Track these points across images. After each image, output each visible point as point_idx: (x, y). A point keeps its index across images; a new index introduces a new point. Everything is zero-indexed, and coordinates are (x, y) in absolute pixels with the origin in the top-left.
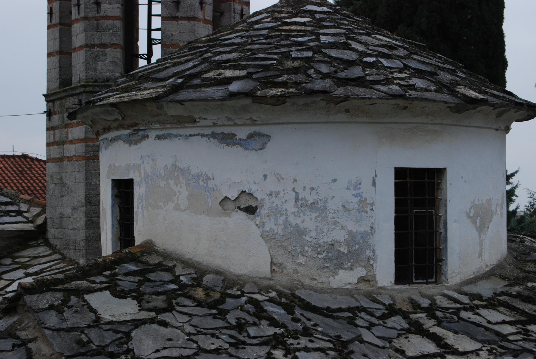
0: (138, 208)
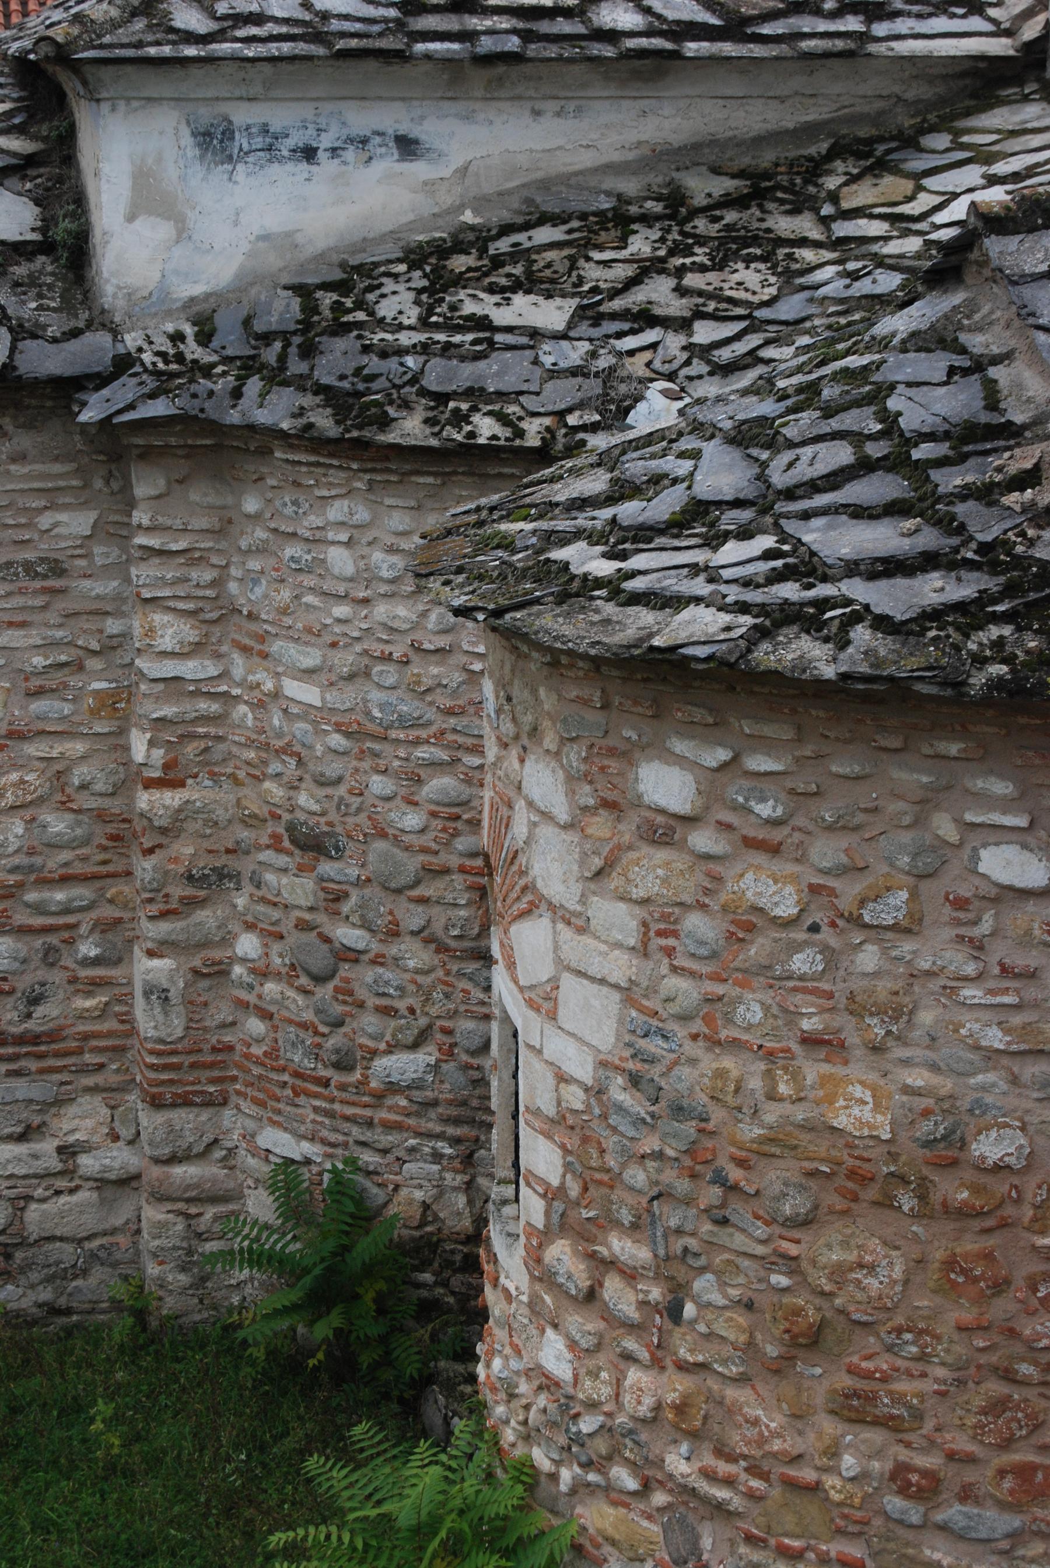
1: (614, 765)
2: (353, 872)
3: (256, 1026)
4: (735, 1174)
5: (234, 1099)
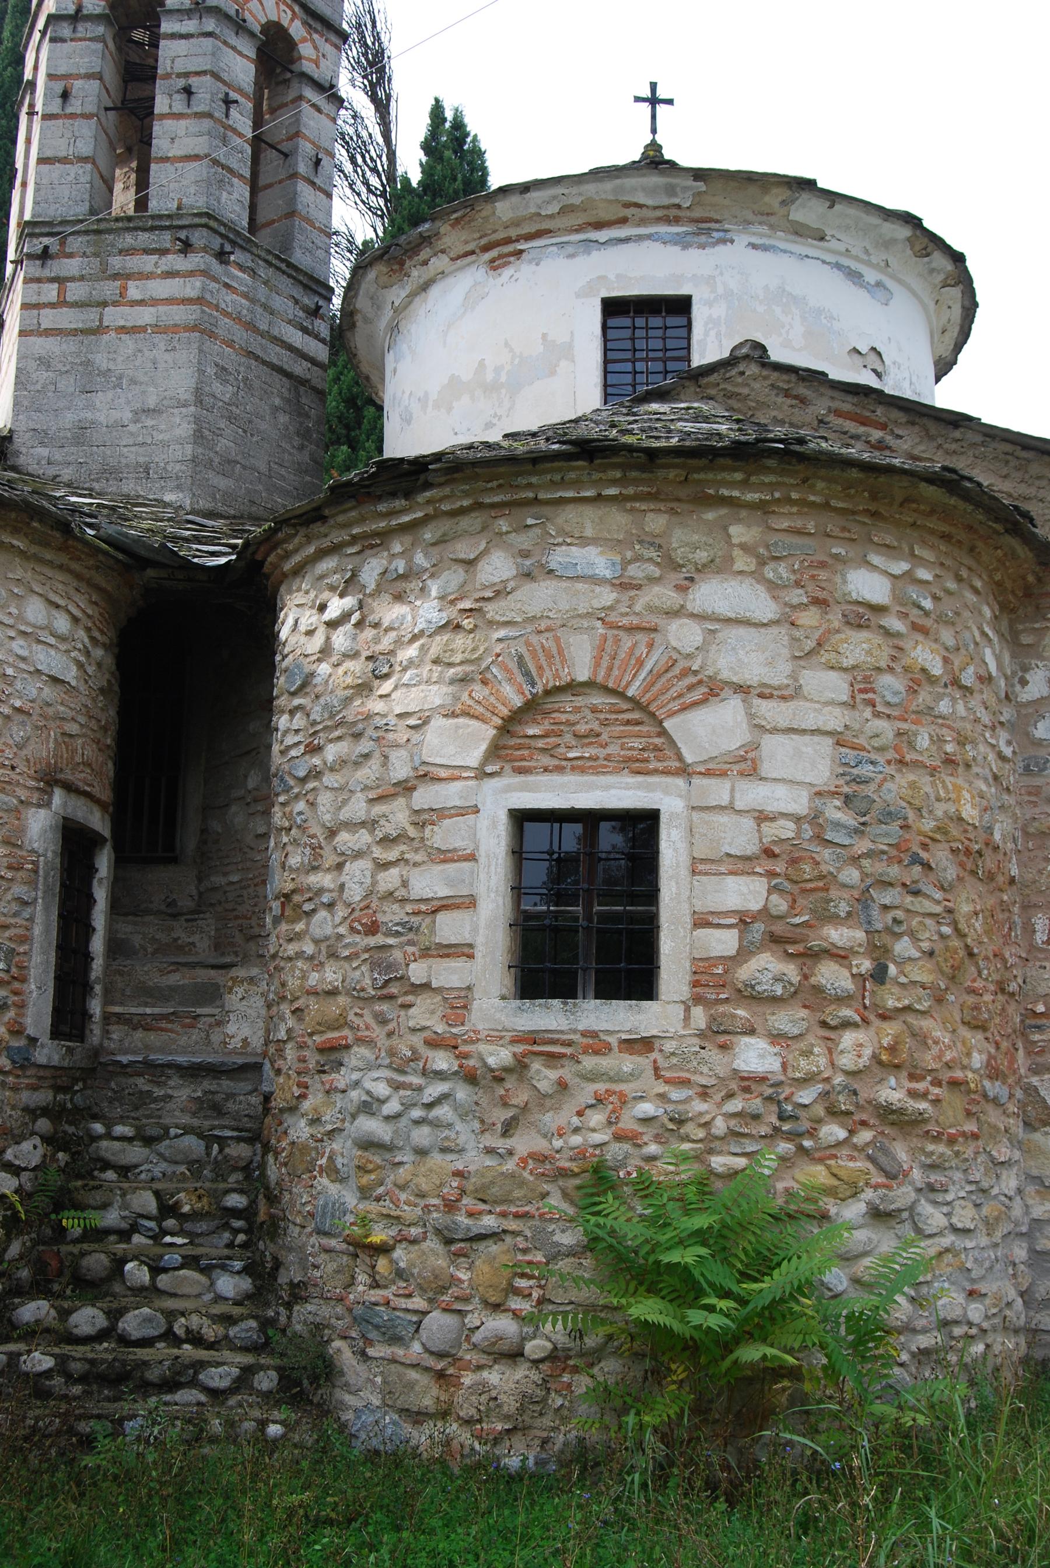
0: (706, 334)
1: (823, 575)
4: (924, 855)
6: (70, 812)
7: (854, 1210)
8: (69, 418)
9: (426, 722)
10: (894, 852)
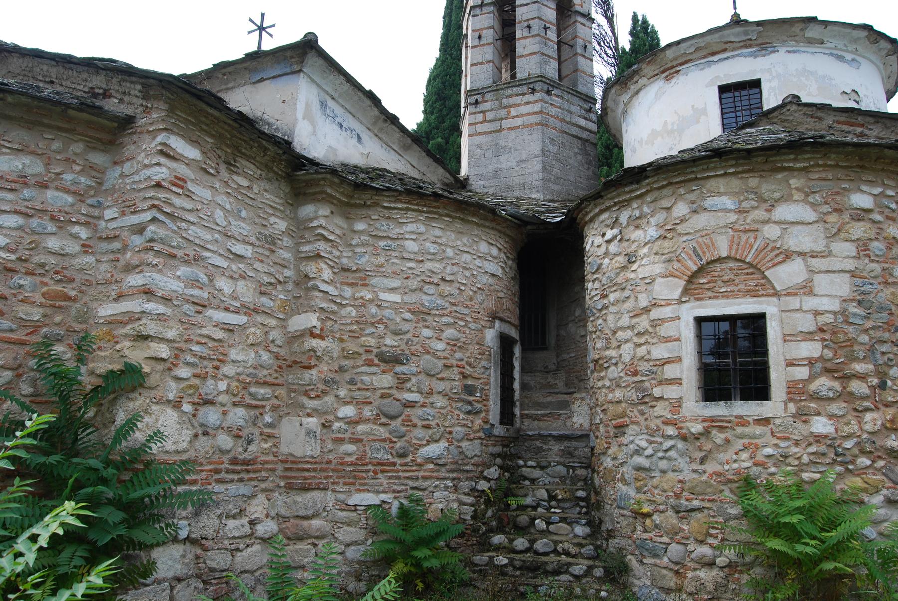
0: (769, 95)
1: (838, 198)
2: (414, 369)
3: (351, 448)
5: (331, 487)
6: (502, 330)
7: (878, 499)
8: (491, 168)
9: (653, 280)
10: (886, 326)
